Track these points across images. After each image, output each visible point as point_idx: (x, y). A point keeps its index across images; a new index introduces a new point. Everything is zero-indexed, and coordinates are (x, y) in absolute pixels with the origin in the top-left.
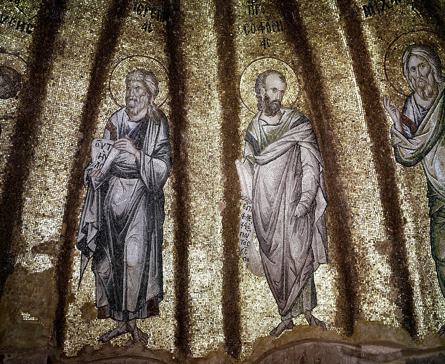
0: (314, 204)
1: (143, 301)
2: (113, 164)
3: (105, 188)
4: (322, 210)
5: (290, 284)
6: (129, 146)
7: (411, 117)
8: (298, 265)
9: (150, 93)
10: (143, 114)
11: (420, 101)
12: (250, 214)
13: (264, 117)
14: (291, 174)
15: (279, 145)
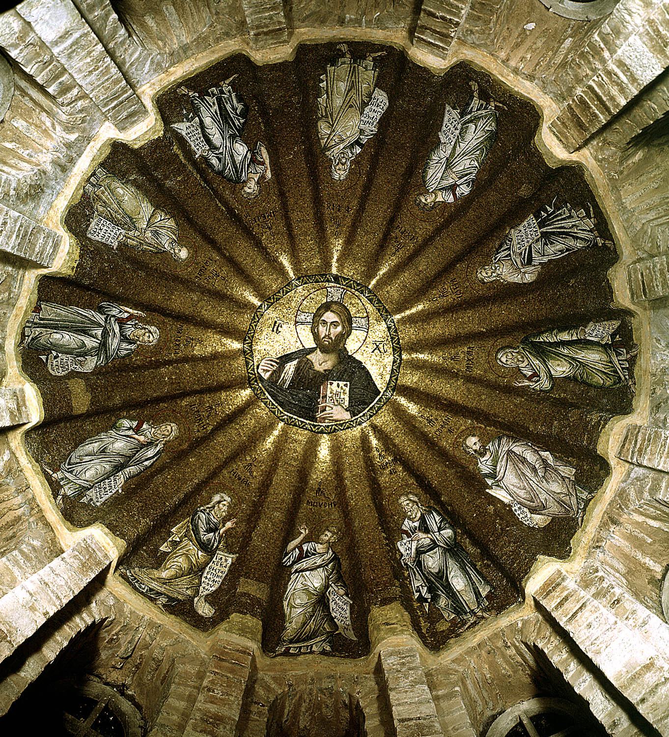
0: (544, 461)
1: (480, 600)
2: (416, 549)
3: (419, 564)
4: (550, 457)
5: (568, 502)
6: (421, 535)
7: (530, 373)
8: (565, 491)
9: (416, 502)
10: (419, 515)
11: (524, 365)
12: (519, 506)
13: (482, 460)
14: (521, 466)
15: (501, 461)
